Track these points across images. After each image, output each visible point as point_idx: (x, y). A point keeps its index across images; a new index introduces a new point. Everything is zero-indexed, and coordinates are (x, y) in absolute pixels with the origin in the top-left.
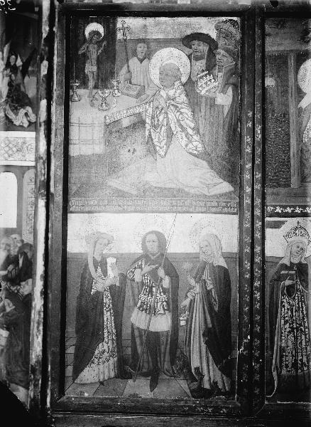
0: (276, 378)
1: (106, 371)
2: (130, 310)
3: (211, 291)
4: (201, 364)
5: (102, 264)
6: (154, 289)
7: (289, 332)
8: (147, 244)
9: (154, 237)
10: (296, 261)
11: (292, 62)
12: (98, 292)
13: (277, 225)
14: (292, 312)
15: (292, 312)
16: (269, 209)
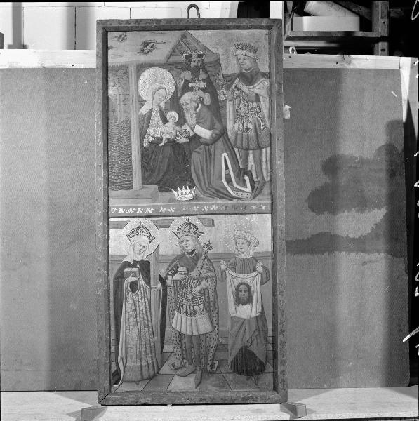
0: (122, 368)
7: (133, 326)
10: (138, 258)
11: (132, 71)
13: (120, 226)
14: (135, 307)
15: (135, 307)
16: (113, 210)
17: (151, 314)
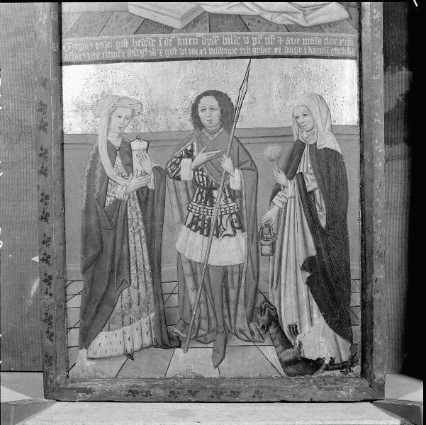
1: (137, 334)
2: (174, 231)
3: (312, 192)
4: (299, 317)
5: (123, 152)
6: (215, 193)
8: (201, 114)
9: (210, 101)
12: (118, 202)
17: (306, 245)
